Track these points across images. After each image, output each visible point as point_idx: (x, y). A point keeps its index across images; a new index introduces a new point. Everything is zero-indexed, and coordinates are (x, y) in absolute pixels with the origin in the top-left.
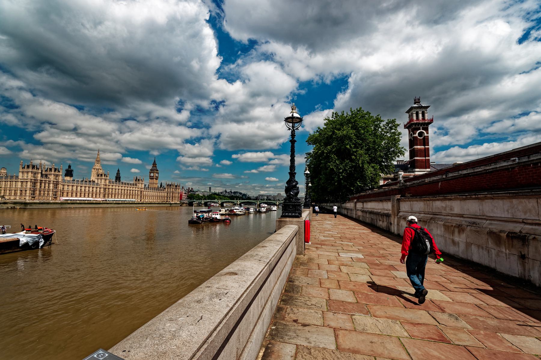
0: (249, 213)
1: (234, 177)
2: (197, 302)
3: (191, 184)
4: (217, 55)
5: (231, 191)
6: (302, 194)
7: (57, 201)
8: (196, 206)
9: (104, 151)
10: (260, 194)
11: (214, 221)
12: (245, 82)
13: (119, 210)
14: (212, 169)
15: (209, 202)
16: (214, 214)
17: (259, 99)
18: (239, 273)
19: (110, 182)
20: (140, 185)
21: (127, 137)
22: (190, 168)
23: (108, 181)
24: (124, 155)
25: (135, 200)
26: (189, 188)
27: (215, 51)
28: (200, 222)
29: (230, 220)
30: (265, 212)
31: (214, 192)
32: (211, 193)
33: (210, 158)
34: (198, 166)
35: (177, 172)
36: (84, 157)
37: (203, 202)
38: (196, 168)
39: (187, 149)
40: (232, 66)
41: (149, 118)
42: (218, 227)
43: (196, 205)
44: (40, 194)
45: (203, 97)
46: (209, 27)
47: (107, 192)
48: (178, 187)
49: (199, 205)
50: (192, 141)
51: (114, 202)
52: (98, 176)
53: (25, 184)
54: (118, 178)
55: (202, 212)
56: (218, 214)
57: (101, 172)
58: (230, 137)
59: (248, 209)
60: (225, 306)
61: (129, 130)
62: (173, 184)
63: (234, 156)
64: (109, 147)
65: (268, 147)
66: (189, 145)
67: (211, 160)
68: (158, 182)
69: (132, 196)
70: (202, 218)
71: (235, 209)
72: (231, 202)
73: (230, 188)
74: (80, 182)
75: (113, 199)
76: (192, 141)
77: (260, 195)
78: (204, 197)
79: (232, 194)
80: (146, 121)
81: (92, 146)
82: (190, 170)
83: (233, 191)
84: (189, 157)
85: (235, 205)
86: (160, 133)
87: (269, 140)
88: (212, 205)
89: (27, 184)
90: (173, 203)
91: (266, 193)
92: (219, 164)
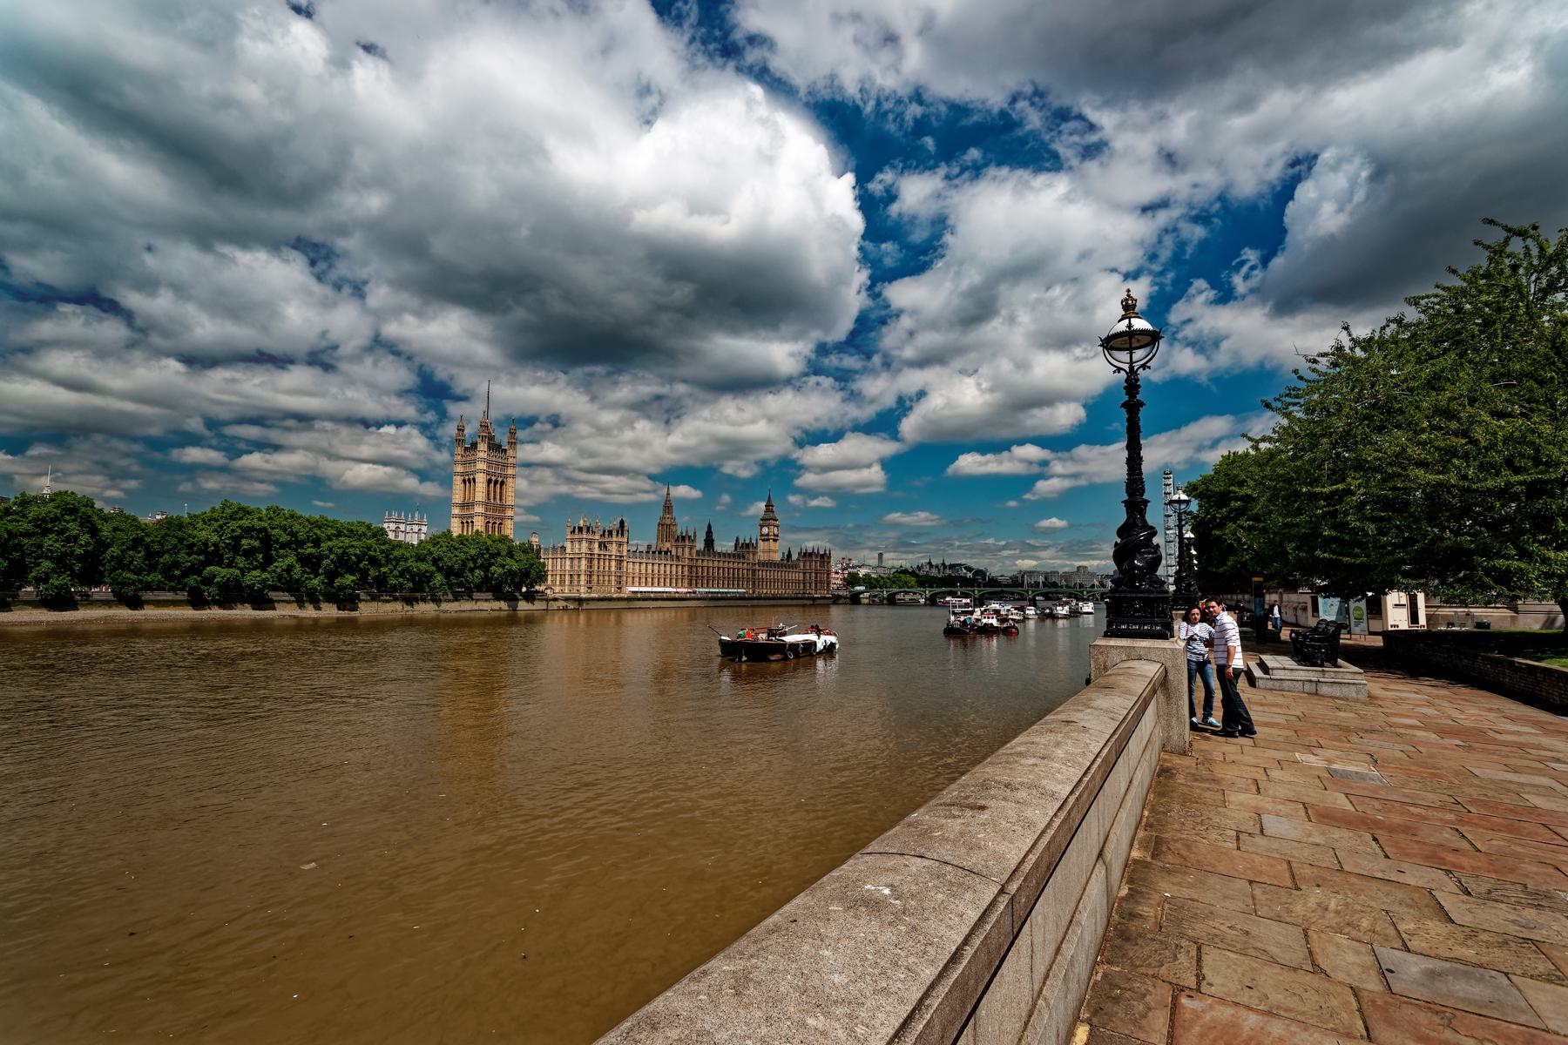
6: (1167, 570)
7: (622, 595)
15: (897, 593)
30: (1065, 617)
53: (576, 562)
74: (644, 554)
83: (947, 564)
89: (579, 562)
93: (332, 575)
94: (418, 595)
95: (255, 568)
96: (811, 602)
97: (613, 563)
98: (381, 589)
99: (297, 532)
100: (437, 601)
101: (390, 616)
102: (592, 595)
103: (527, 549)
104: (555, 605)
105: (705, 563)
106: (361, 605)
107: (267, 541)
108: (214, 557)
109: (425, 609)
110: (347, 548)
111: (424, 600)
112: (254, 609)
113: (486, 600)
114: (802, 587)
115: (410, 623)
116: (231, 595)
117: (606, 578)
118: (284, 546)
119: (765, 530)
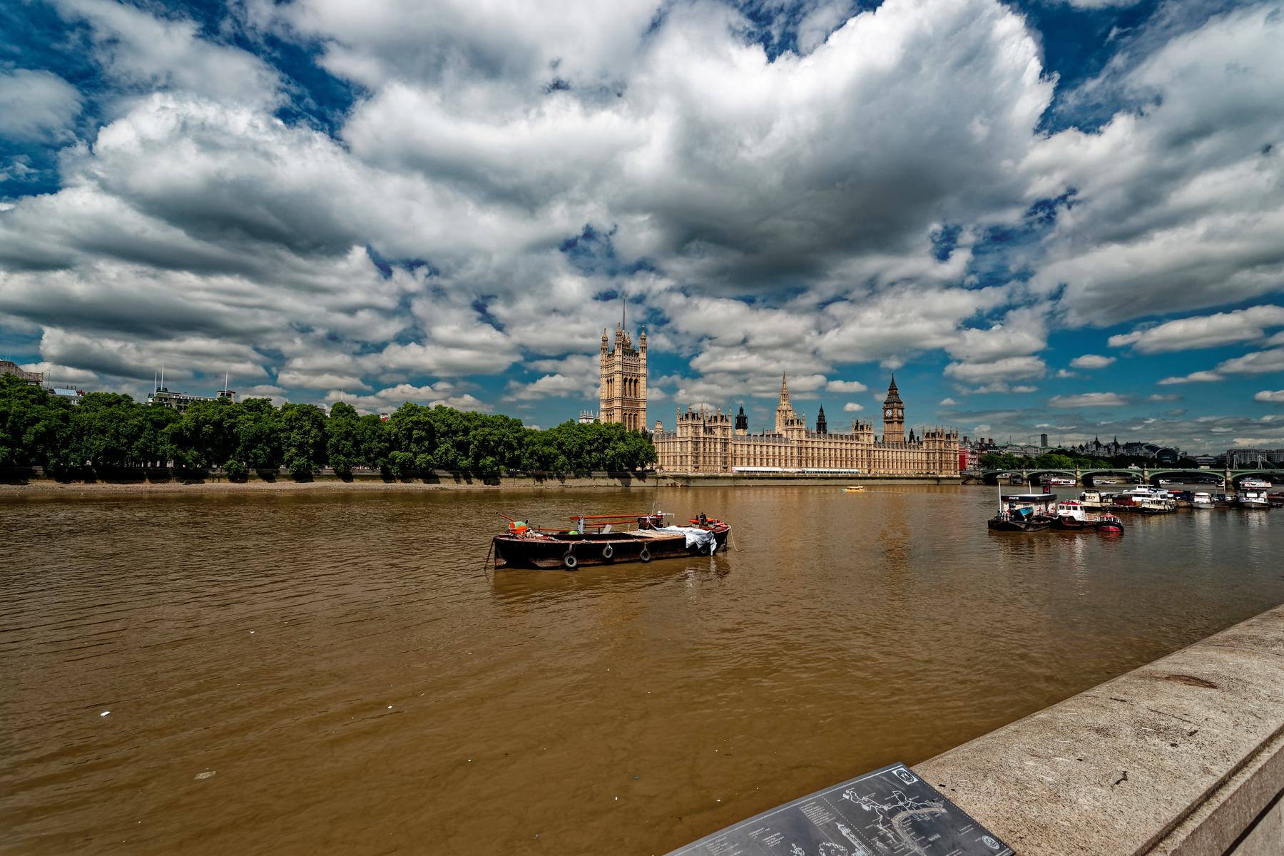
0: (1193, 509)
1: (1122, 400)
2: (1097, 731)
3: (986, 428)
4: (1041, 76)
5: (1115, 444)
7: (728, 474)
8: (1006, 485)
9: (795, 374)
10: (1235, 447)
11: (1066, 527)
12: (1142, 114)
13: (828, 490)
14: (1046, 386)
15: (1043, 473)
16: (1062, 508)
17: (1203, 147)
18: (1224, 683)
19: (807, 433)
20: (866, 437)
21: (832, 339)
22: (983, 390)
23: (804, 433)
24: (830, 378)
25: (857, 470)
26: (982, 439)
27: (1035, 66)
28: (1023, 526)
29: (1119, 525)
31: (1056, 446)
32: (1049, 450)
33: (1037, 357)
34: (1004, 381)
35: (947, 401)
36: (761, 389)
37: (1025, 475)
38: (998, 388)
39: (969, 342)
40: (1091, 85)
41: (873, 288)
42: (1079, 543)
43: (1004, 482)
44: (704, 462)
45: (1003, 201)
46: (1010, 13)
47: (804, 455)
48: (952, 439)
49: (1015, 482)
50: (980, 322)
51: (819, 475)
52: (787, 424)
54: (822, 426)
55: (1023, 500)
56: (1075, 508)
57: (791, 415)
58: (1103, 286)
59: (1188, 496)
60: (1196, 767)
61: (835, 324)
62: (940, 430)
63: (1117, 341)
64: (801, 366)
65: (1258, 291)
66: (973, 334)
67: (1042, 364)
68: (906, 427)
69: (852, 461)
70: (1027, 516)
71: (1137, 495)
72: (1119, 474)
73: (1113, 435)
74: (758, 438)
75: (816, 470)
76: (980, 322)
77: (1232, 453)
78: (1027, 462)
79: (1121, 451)
80: (870, 295)
81: (773, 367)
82: (982, 395)
84: (978, 362)
85: (1133, 481)
86: (898, 316)
87: (1259, 267)
88: (1055, 483)
90: (944, 476)
91: (1262, 445)
92: (1069, 369)
93: (478, 457)
94: (546, 473)
95: (423, 452)
96: (935, 482)
97: (718, 446)
98: (516, 467)
99: (451, 424)
100: (562, 478)
101: (523, 490)
102: (699, 474)
103: (647, 437)
104: (664, 483)
105: (816, 445)
106: (502, 481)
107: (431, 431)
108: (395, 444)
109: (552, 485)
110: (487, 435)
111: (551, 477)
112: (425, 483)
113: (603, 478)
114: (925, 467)
115: (541, 496)
116: (408, 472)
117: (712, 459)
118: (444, 435)
119: (889, 413)
